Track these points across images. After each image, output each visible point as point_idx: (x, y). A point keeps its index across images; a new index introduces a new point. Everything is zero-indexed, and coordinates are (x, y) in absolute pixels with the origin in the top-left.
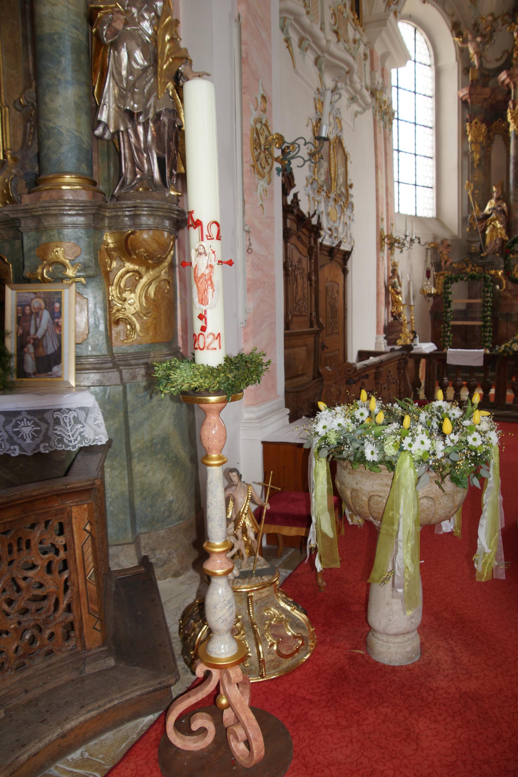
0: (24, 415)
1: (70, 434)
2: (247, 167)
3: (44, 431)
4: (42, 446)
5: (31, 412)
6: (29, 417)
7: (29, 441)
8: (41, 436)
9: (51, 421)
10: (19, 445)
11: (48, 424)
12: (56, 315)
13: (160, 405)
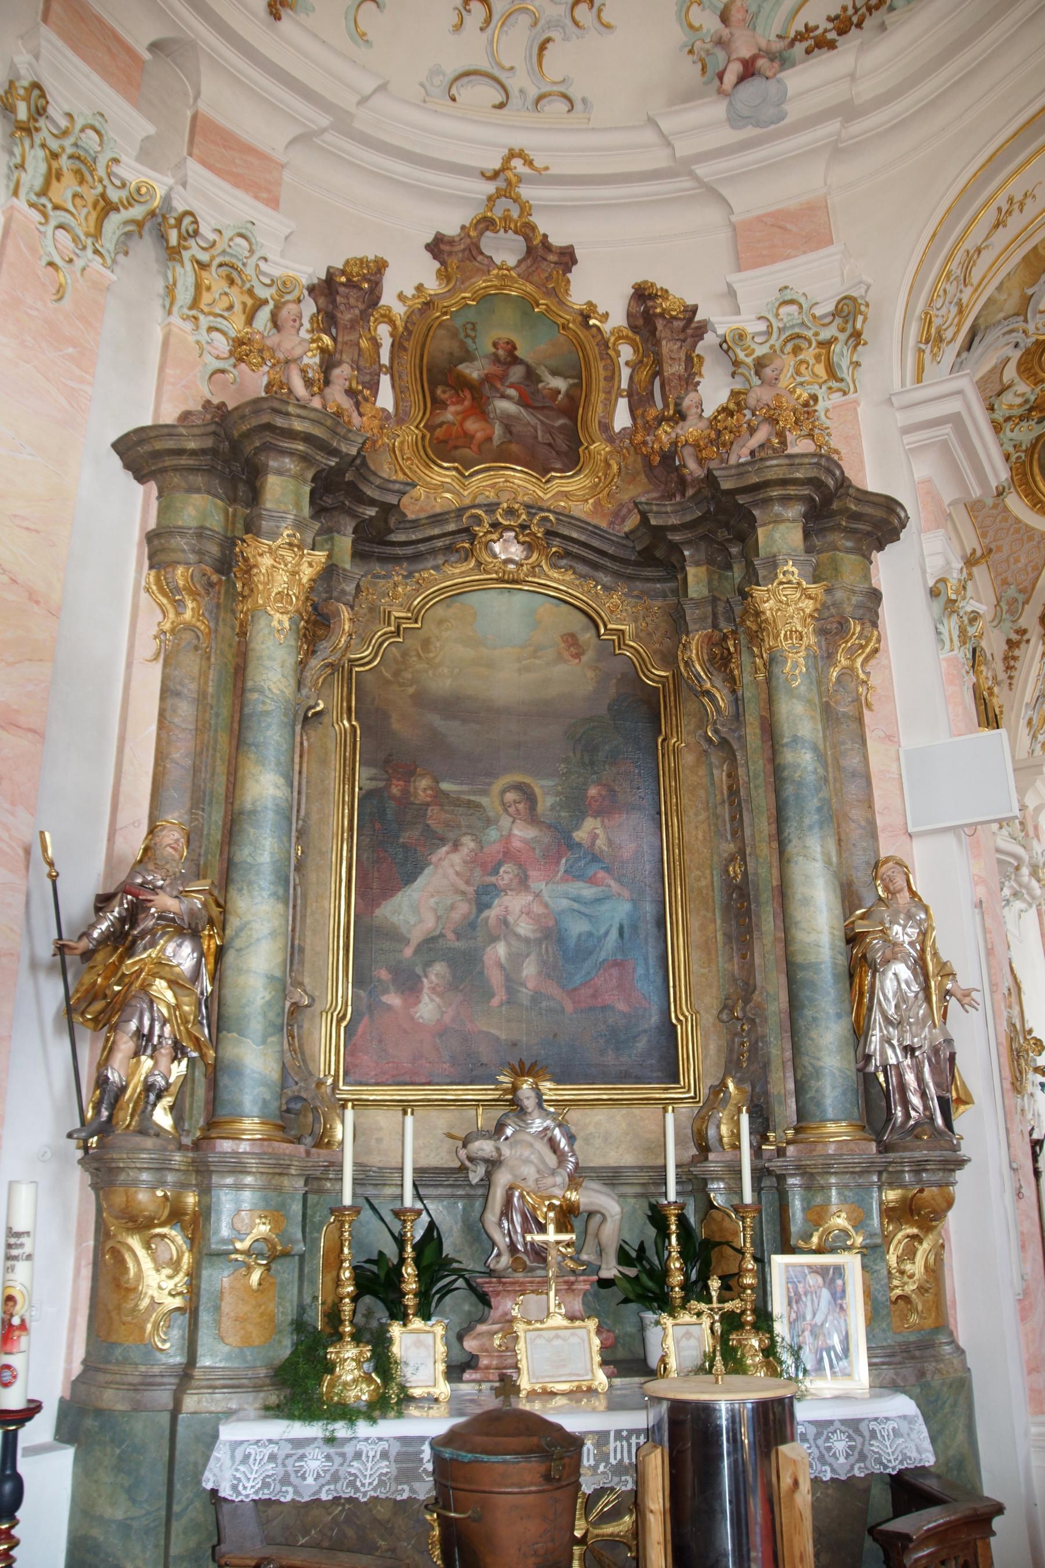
0: (837, 1425)
1: (890, 1451)
2: (1007, 1085)
3: (859, 1446)
4: (857, 1466)
5: (843, 1422)
6: (843, 1428)
7: (842, 1460)
8: (856, 1454)
9: (867, 1434)
10: (831, 1465)
11: (863, 1436)
12: (838, 1295)
13: (953, 1413)
